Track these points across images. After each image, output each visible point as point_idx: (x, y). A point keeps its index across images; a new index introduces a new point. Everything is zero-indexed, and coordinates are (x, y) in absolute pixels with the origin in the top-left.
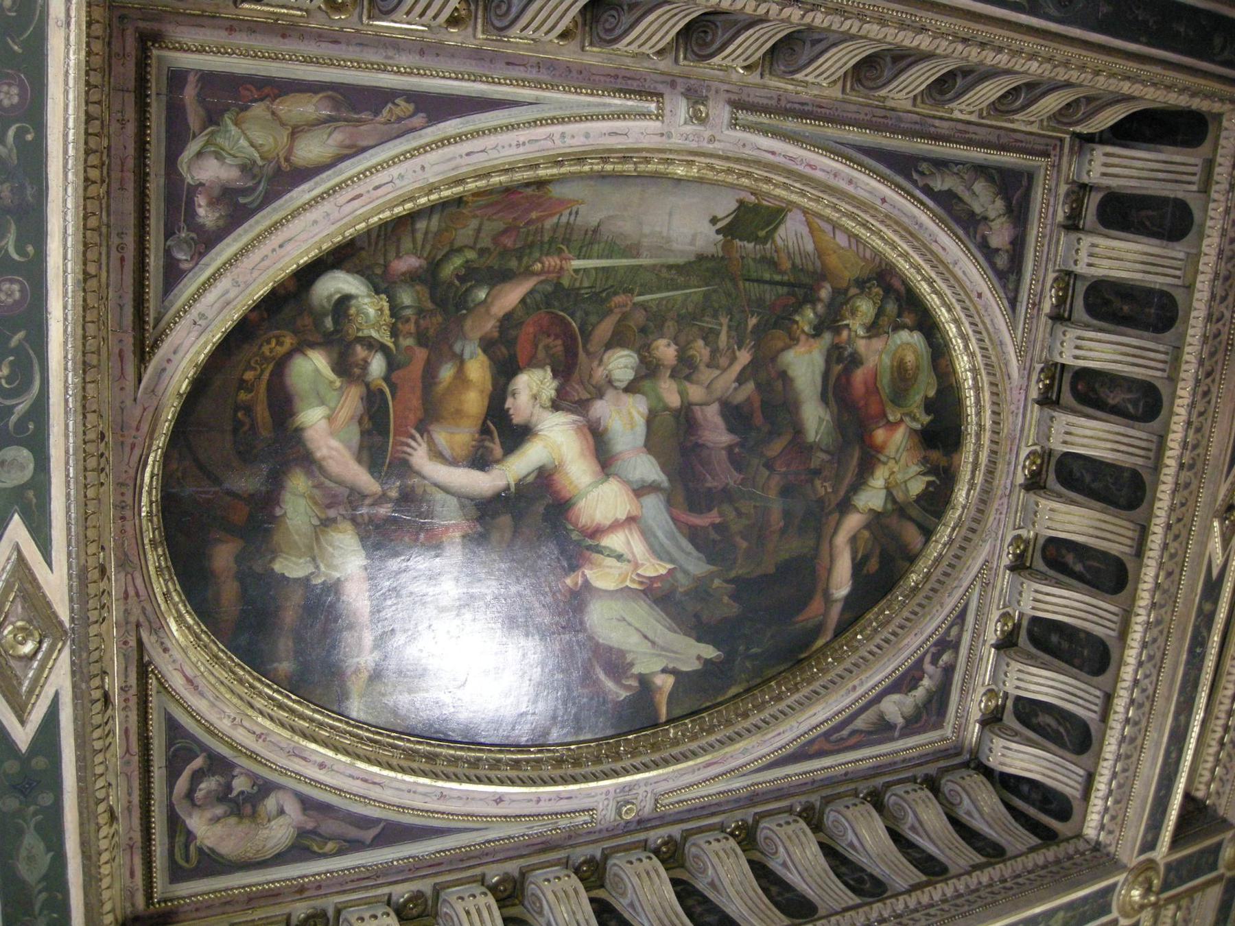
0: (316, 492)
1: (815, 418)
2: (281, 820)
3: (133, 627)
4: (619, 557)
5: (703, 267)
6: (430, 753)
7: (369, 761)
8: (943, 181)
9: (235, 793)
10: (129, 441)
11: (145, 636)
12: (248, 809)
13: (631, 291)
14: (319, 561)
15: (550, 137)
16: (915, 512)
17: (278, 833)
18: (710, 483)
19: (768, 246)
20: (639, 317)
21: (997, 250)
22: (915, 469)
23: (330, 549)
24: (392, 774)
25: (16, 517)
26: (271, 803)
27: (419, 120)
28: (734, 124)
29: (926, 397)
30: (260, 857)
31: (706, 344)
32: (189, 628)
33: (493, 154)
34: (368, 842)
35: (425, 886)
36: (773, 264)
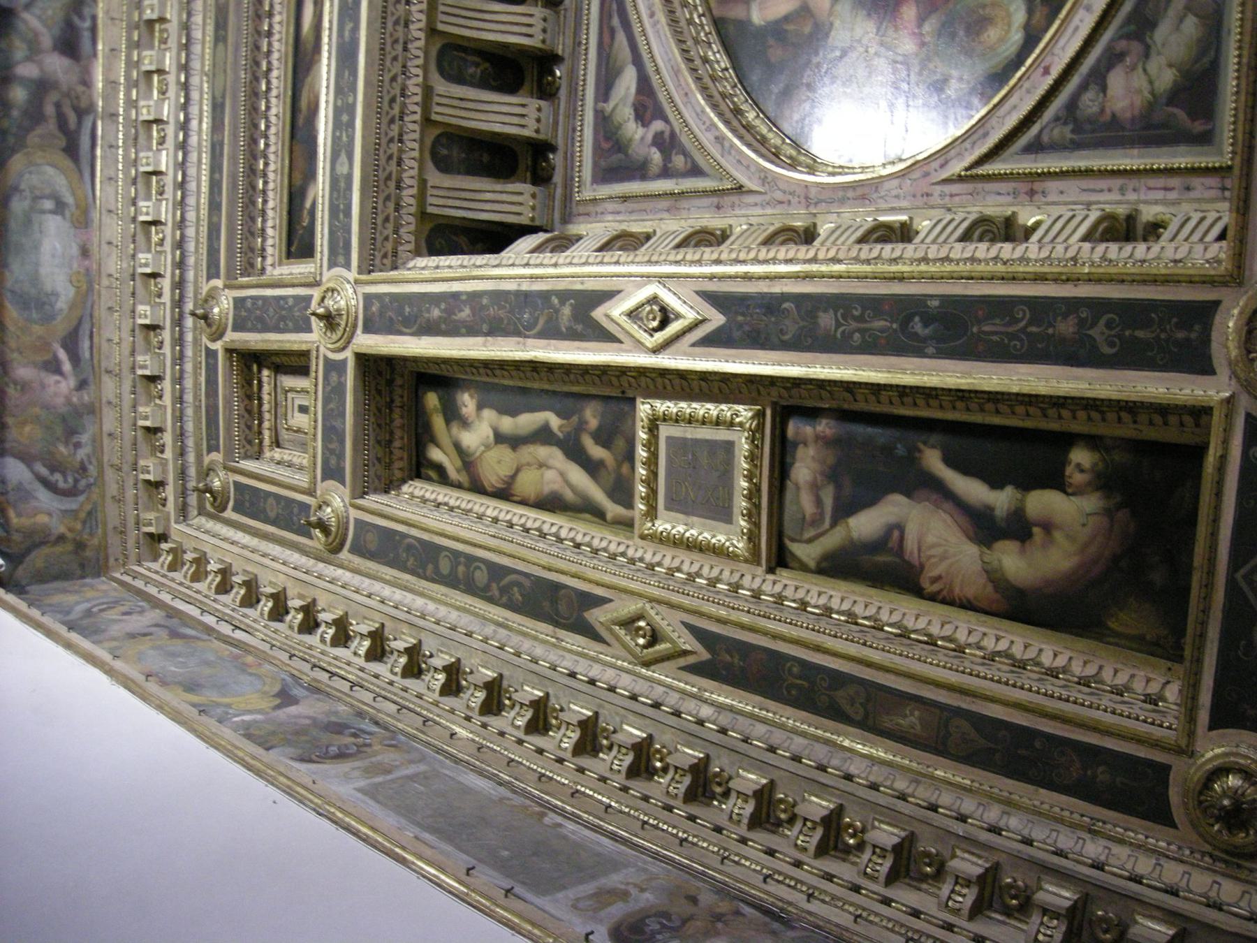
21: (1104, 89)
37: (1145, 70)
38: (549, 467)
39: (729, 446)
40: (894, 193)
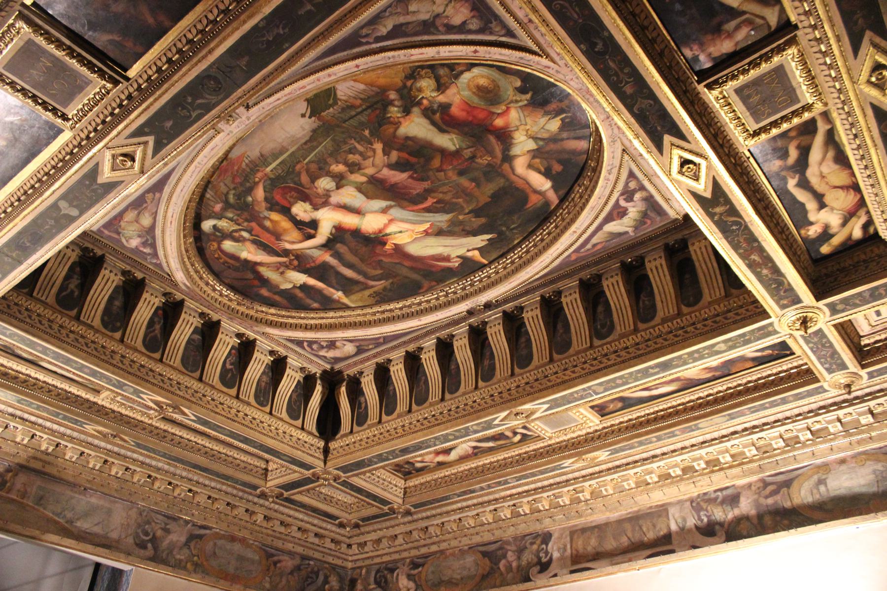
1: (447, 141)
4: (401, 232)
5: (315, 136)
8: (385, 26)
13: (299, 162)
15: (196, 167)
16: (565, 135)
17: (350, 349)
18: (415, 192)
19: (340, 103)
20: (313, 167)
21: (464, 23)
22: (543, 121)
27: (157, 195)
28: (248, 107)
29: (516, 88)
31: (354, 154)
33: (188, 185)
36: (352, 107)
37: (444, 12)
38: (821, 173)
39: (738, 91)
40: (576, 80)
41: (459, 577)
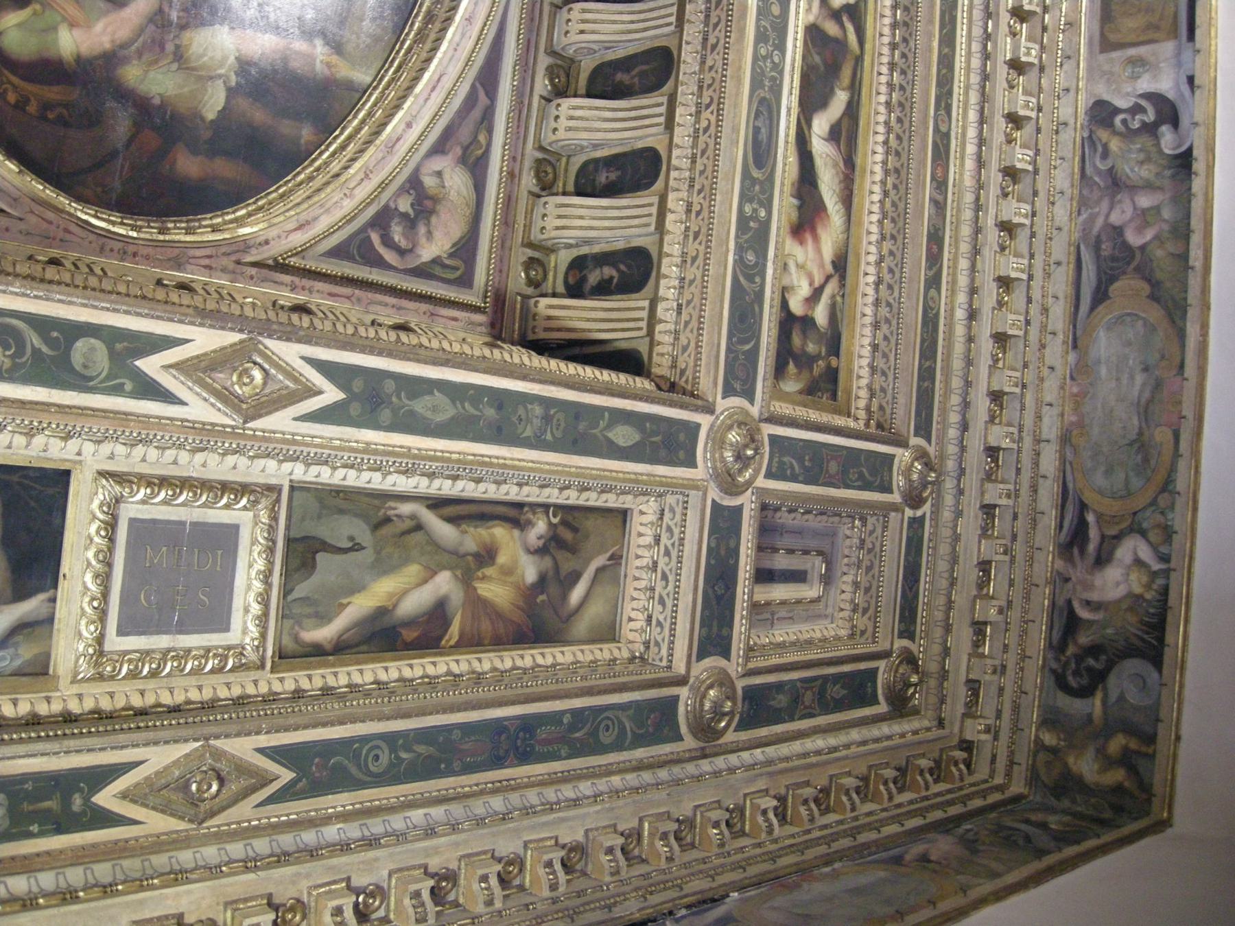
0: (145, 58)
2: (446, 176)
3: (239, 268)
6: (424, 18)
7: (416, 79)
9: (411, 212)
10: (61, 234)
11: (249, 259)
12: (428, 203)
14: (213, 74)
17: (457, 182)
23: (205, 59)
24: (435, 62)
25: (137, 363)
26: (429, 181)
30: (473, 203)
32: (250, 215)
34: (489, 102)
35: (544, 61)
41: (1139, 379)
